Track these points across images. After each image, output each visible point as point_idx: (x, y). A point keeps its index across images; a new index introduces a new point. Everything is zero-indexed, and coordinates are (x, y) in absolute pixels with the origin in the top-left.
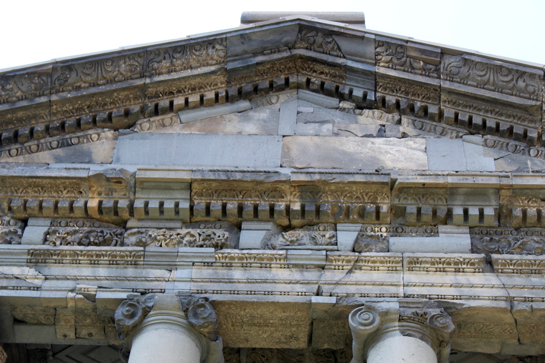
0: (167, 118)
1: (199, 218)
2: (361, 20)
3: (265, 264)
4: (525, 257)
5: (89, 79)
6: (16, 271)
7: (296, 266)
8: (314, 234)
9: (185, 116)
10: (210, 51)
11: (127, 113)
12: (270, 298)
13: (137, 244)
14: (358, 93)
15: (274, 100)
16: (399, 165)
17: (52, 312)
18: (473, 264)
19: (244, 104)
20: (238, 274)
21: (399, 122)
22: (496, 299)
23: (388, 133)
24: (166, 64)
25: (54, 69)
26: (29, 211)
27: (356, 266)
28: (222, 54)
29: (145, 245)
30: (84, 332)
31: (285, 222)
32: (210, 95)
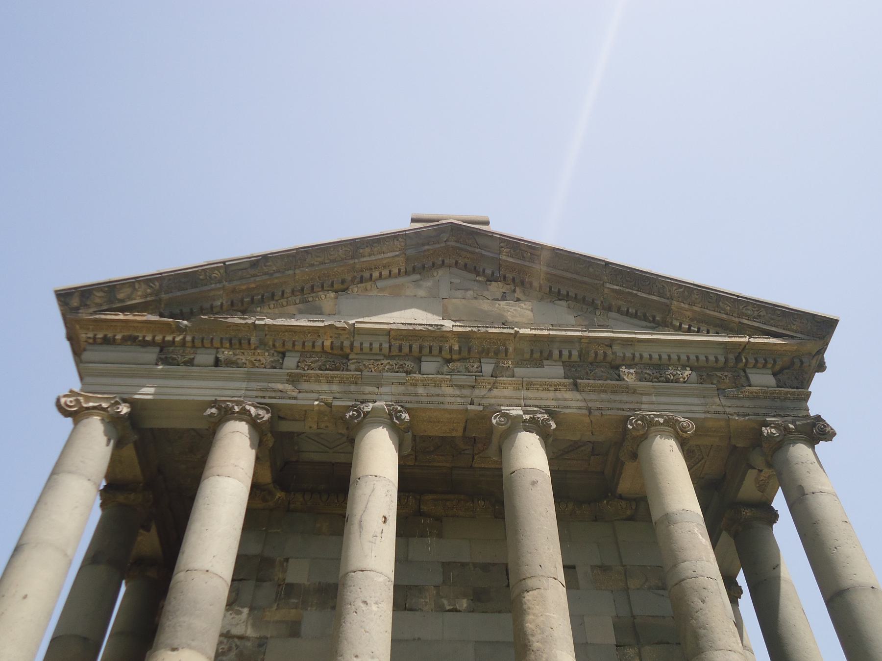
1: (394, 354)
2: (486, 219)
3: (438, 385)
4: (597, 382)
5: (319, 259)
6: (280, 386)
7: (456, 386)
8: (468, 365)
9: (380, 284)
10: (396, 242)
11: (343, 282)
12: (442, 406)
13: (356, 370)
14: (488, 272)
15: (435, 274)
17: (305, 413)
19: (417, 277)
20: (421, 390)
21: (514, 291)
22: (580, 408)
23: (508, 298)
24: (368, 250)
26: (286, 347)
27: (494, 386)
28: (403, 244)
29: (361, 371)
30: (323, 425)
31: (448, 357)
32: (395, 271)
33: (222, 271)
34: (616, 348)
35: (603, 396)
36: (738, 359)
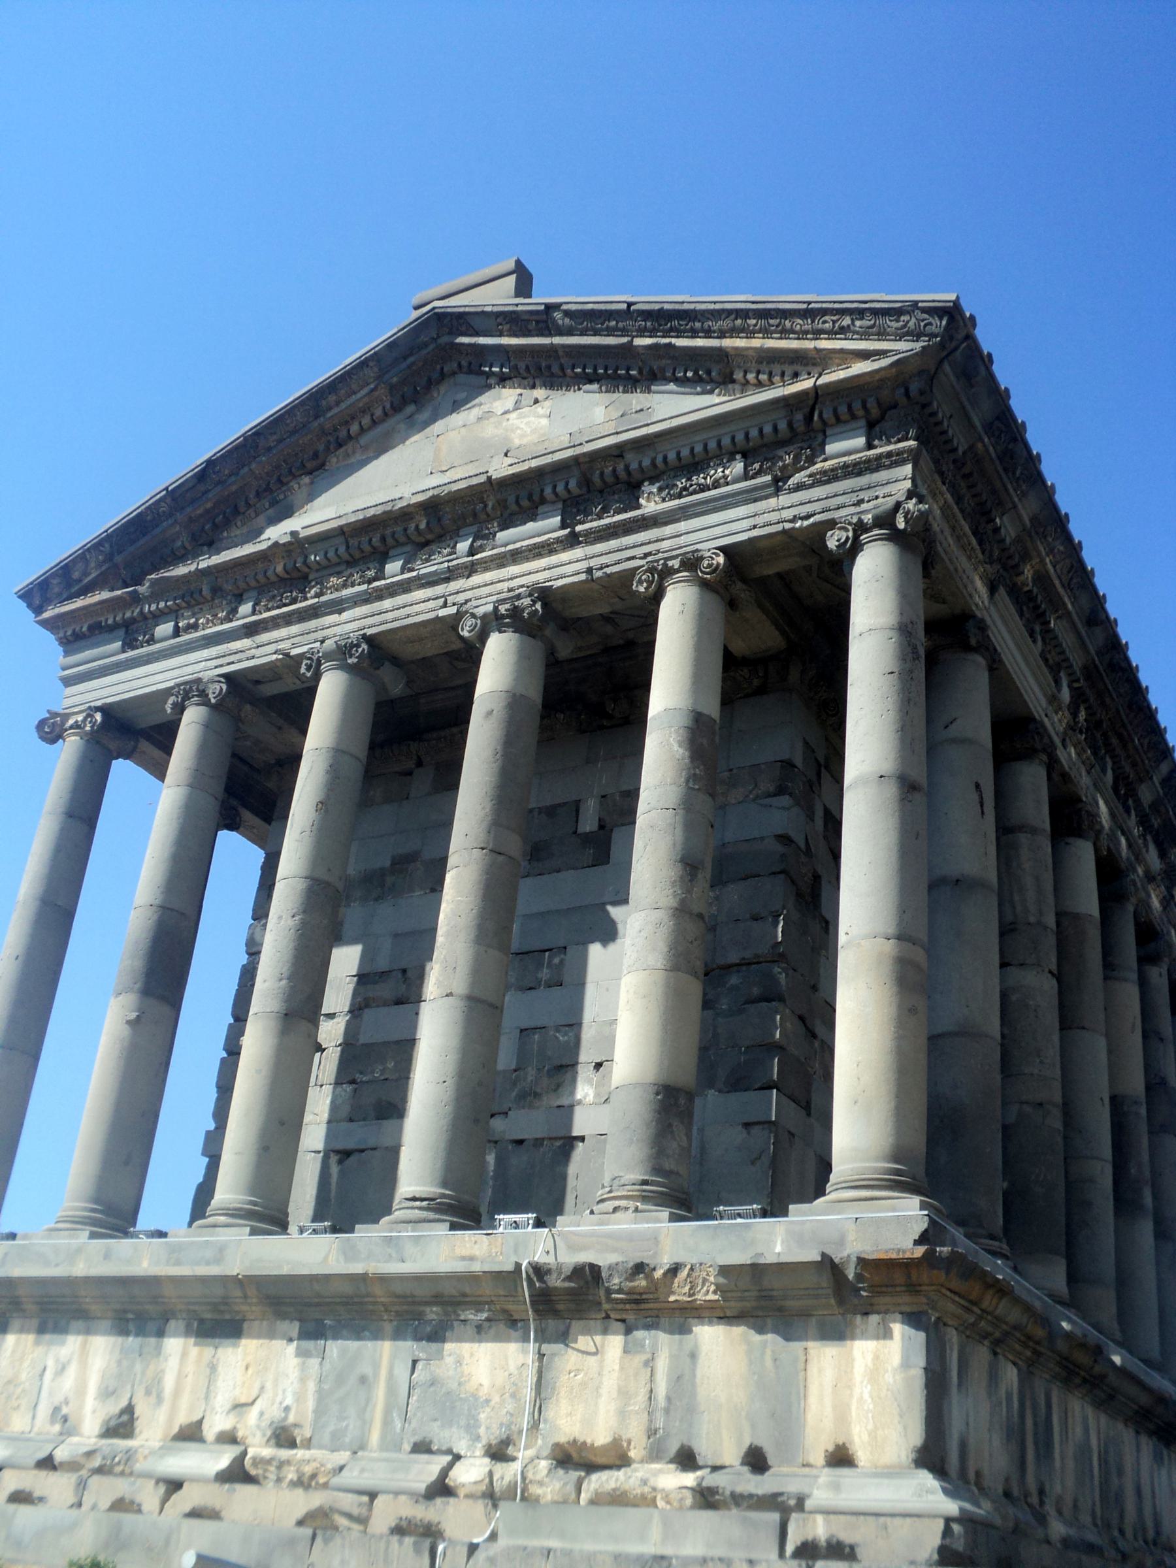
0: (349, 447)
5: (275, 437)
9: (364, 440)
10: (366, 371)
11: (316, 455)
16: (525, 441)
18: (562, 542)
19: (411, 408)
20: (387, 604)
24: (332, 398)
25: (246, 439)
27: (471, 570)
28: (376, 369)
32: (378, 412)
33: (169, 500)
34: (629, 456)
35: (613, 544)
36: (809, 418)
